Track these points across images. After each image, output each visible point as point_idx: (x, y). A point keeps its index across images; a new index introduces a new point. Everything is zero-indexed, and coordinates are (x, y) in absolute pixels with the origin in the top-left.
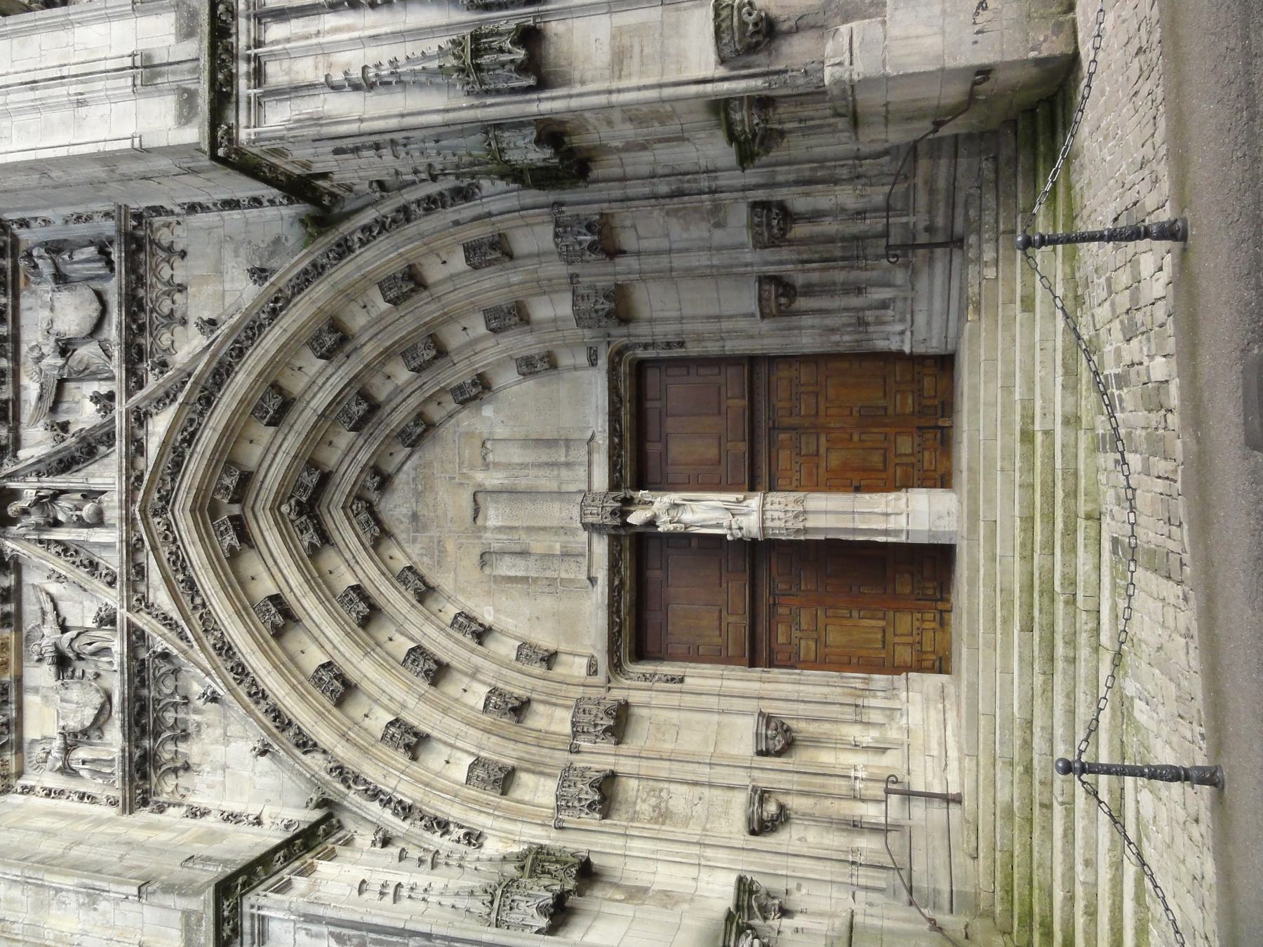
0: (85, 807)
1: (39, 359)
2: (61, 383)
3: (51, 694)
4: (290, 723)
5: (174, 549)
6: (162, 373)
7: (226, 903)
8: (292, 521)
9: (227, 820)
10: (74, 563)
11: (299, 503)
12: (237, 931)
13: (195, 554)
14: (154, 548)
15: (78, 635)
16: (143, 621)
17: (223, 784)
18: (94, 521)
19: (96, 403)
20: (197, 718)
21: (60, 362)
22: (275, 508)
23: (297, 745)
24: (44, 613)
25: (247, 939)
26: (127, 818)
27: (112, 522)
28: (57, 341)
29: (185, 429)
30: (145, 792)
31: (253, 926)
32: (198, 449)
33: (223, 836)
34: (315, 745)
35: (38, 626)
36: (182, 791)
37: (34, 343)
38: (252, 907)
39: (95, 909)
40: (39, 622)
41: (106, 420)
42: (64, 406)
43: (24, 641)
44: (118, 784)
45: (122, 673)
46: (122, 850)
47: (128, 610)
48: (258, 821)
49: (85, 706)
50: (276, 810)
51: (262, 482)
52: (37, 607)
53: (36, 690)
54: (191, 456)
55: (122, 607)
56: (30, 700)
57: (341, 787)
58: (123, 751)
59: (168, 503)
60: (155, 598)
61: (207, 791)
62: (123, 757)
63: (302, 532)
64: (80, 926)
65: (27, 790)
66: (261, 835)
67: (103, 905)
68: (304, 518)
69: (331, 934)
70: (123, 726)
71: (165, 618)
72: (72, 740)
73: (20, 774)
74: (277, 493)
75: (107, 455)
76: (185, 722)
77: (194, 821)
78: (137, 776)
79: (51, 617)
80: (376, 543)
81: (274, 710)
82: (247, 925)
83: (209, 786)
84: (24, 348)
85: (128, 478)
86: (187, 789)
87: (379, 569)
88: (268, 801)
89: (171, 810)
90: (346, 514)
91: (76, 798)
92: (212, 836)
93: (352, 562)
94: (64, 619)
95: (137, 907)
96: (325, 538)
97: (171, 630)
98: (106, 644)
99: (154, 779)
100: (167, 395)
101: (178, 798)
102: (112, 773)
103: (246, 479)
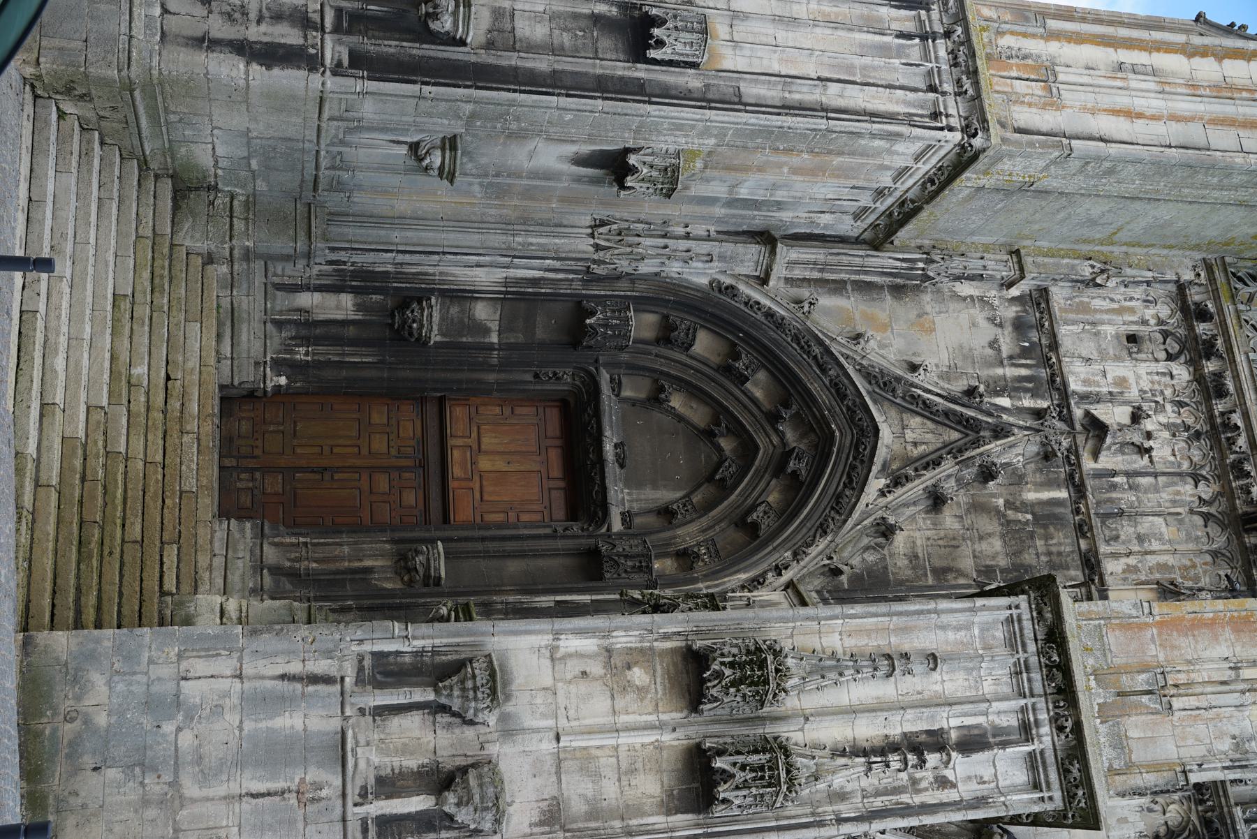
7: (1082, 805)
12: (1064, 772)
25: (1050, 758)
30: (1202, 802)
31: (1047, 776)
36: (1157, 807)
38: (1051, 798)
39: (1234, 737)
61: (1126, 813)
64: (1247, 713)
67: (1225, 745)
69: (954, 786)
78: (1217, 825)
82: (1054, 776)
86: (1150, 810)
95: (1186, 753)
99: (1194, 818)
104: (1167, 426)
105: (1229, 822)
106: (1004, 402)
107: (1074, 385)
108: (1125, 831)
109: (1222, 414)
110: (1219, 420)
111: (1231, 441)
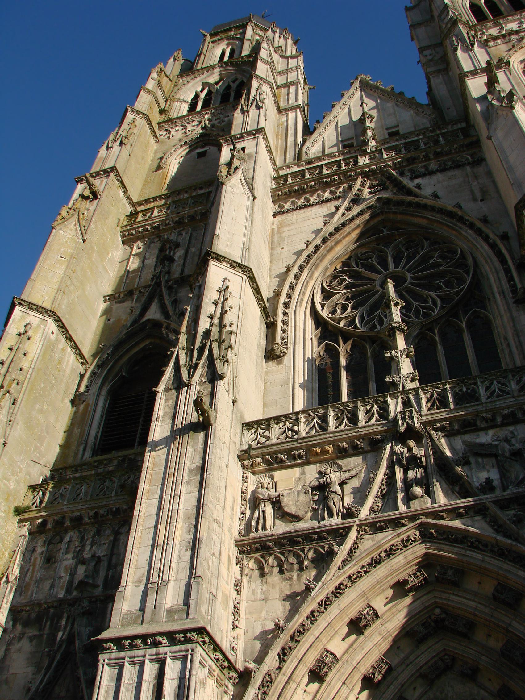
0: (237, 515)
1: (507, 440)
2: (495, 456)
3: (302, 483)
4: (298, 641)
5: (400, 547)
6: (514, 522)
8: (430, 617)
9: (235, 607)
10: (382, 484)
11: (443, 620)
13: (399, 560)
14: (398, 535)
15: (339, 495)
16: (353, 534)
17: (255, 600)
18: (410, 495)
19: (485, 482)
20: (295, 577)
21: (507, 454)
22: (436, 605)
23: (283, 649)
24: (349, 471)
26: (233, 542)
27: (412, 506)
28: (520, 449)
29: (479, 542)
32: (468, 552)
33: (226, 608)
34: (284, 661)
35: (341, 469)
37: (516, 433)
40: (344, 469)
41: (476, 490)
42: (480, 460)
43: (331, 461)
44: (252, 535)
45: (319, 528)
46: (217, 554)
47: (358, 525)
48: (234, 627)
49: (297, 506)
50: (242, 638)
51: (453, 594)
52: (352, 466)
53: (303, 473)
54: (462, 548)
55: (360, 521)
56: (297, 471)
57: (259, 682)
58: (272, 535)
59: (429, 538)
60: (368, 539)
61: (251, 590)
62: (269, 536)
63: (423, 625)
65: (245, 479)
66: (227, 632)
68: (433, 624)
70: (287, 533)
71: (355, 549)
72: (276, 503)
73: (253, 473)
74: (448, 605)
75: (453, 492)
76: (292, 570)
77: (233, 585)
79: (347, 475)
80: (423, 676)
81: (304, 630)
83: (254, 590)
84: (511, 428)
85: (441, 511)
86: (251, 577)
87: (405, 683)
88: (247, 631)
89: (238, 568)
90: (440, 652)
91: (242, 510)
92: (226, 599)
93: (407, 662)
94: (346, 483)
96: (421, 640)
97: (348, 554)
98: (335, 514)
100: (500, 526)
101: (246, 571)
102: (257, 530)
103: (456, 584)
104: (92, 547)
105: (256, 540)
106: (60, 634)
107: (61, 595)
108: (259, 591)
109: (89, 519)
110: (92, 520)
111: (102, 516)
